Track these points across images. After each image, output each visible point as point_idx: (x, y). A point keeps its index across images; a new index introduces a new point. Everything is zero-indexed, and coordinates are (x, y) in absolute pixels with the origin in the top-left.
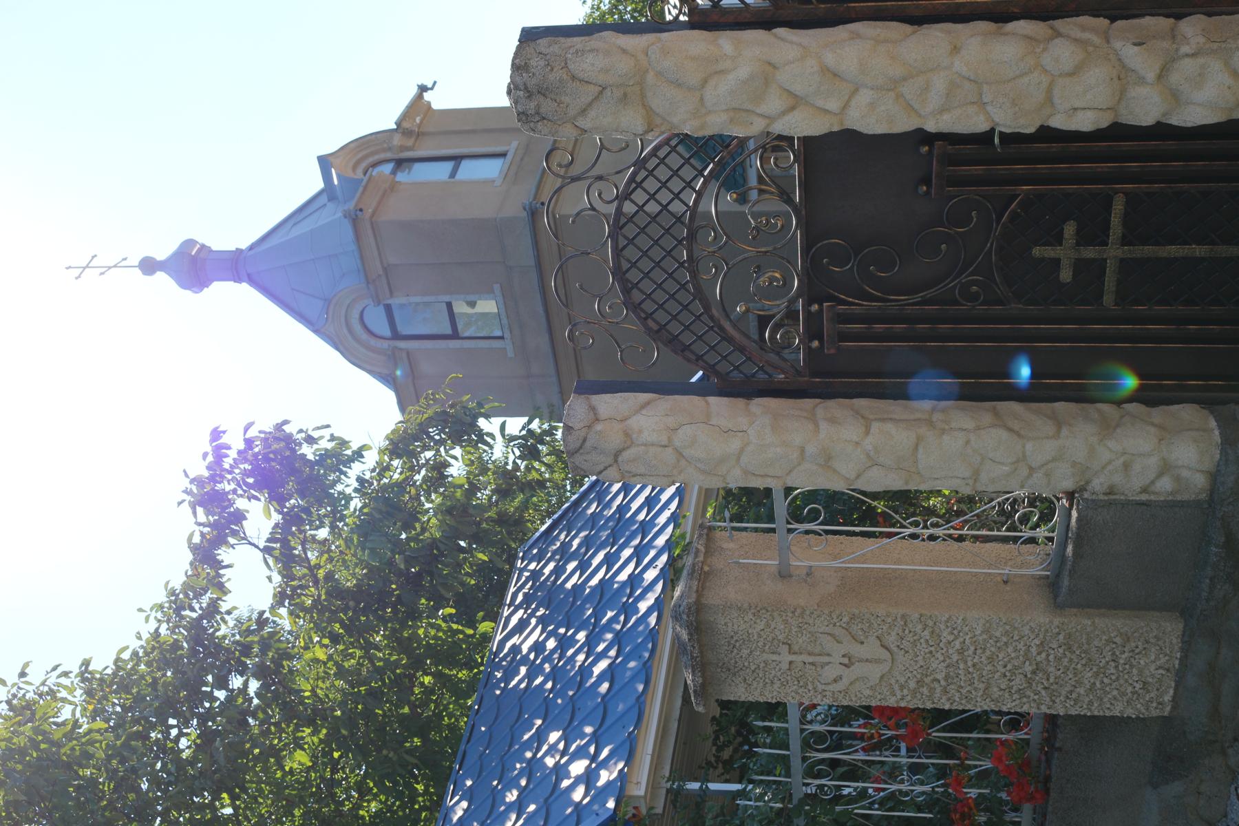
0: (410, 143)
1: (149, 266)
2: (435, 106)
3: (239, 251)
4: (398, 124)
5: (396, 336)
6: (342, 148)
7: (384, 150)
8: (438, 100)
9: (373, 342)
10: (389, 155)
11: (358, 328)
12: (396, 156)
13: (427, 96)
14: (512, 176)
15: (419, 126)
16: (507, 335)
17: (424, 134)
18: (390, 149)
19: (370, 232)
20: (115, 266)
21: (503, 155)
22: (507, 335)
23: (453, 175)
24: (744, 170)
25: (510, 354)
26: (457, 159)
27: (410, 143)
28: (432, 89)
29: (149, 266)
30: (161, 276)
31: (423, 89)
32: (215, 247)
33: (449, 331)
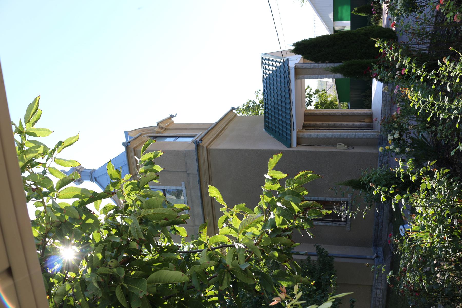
0: (161, 131)
2: (175, 122)
3: (94, 170)
4: (158, 124)
6: (135, 130)
8: (176, 121)
10: (152, 135)
12: (155, 135)
13: (173, 119)
15: (167, 126)
17: (168, 129)
18: (153, 133)
19: (133, 152)
24: (291, 132)
27: (161, 131)
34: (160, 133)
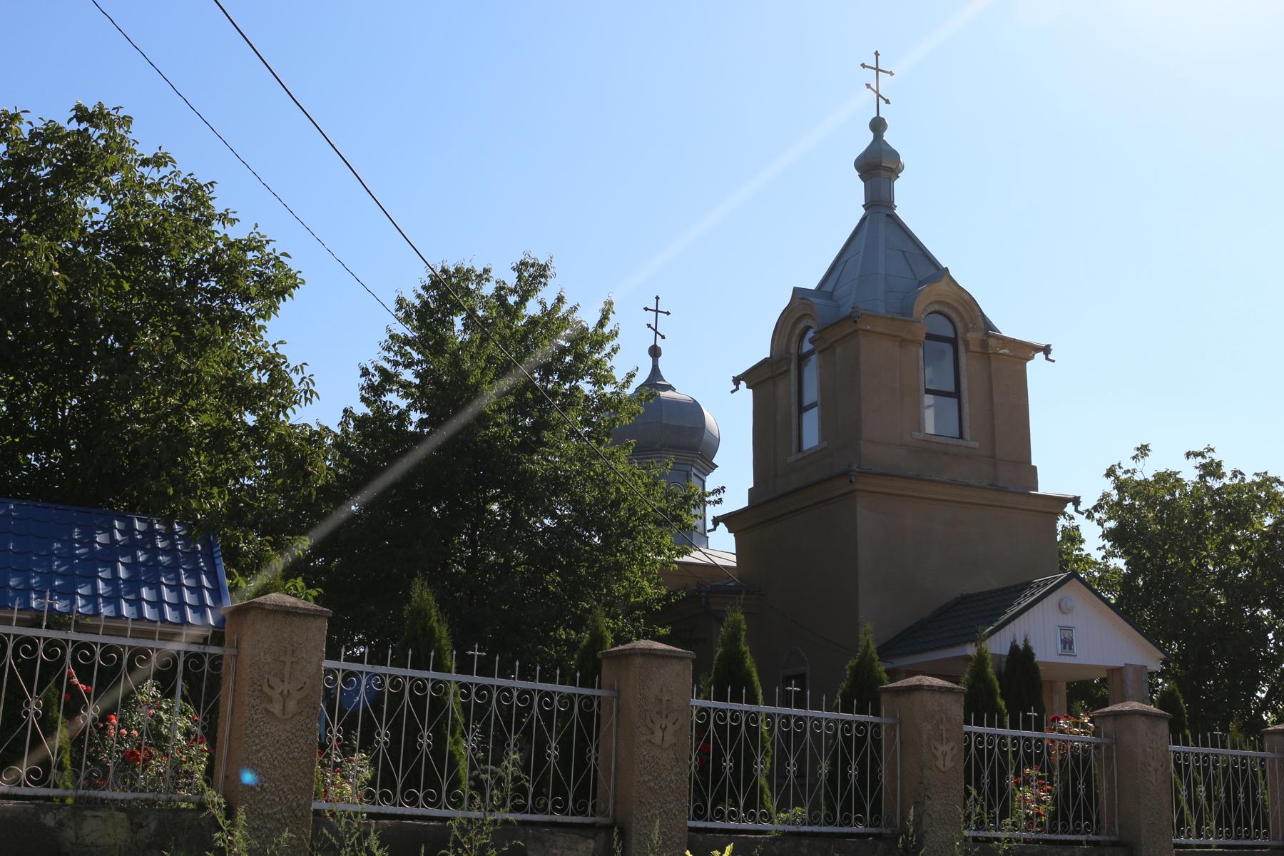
1: (878, 125)
2: (1029, 365)
5: (802, 359)
7: (966, 326)
8: (1035, 368)
9: (794, 339)
10: (960, 331)
11: (801, 326)
14: (928, 449)
16: (800, 455)
20: (879, 96)
21: (961, 437)
22: (800, 455)
23: (928, 391)
25: (791, 459)
26: (957, 394)
28: (1047, 359)
29: (878, 125)
30: (869, 137)
31: (1047, 350)
32: (898, 185)
33: (807, 401)
34: (968, 350)
